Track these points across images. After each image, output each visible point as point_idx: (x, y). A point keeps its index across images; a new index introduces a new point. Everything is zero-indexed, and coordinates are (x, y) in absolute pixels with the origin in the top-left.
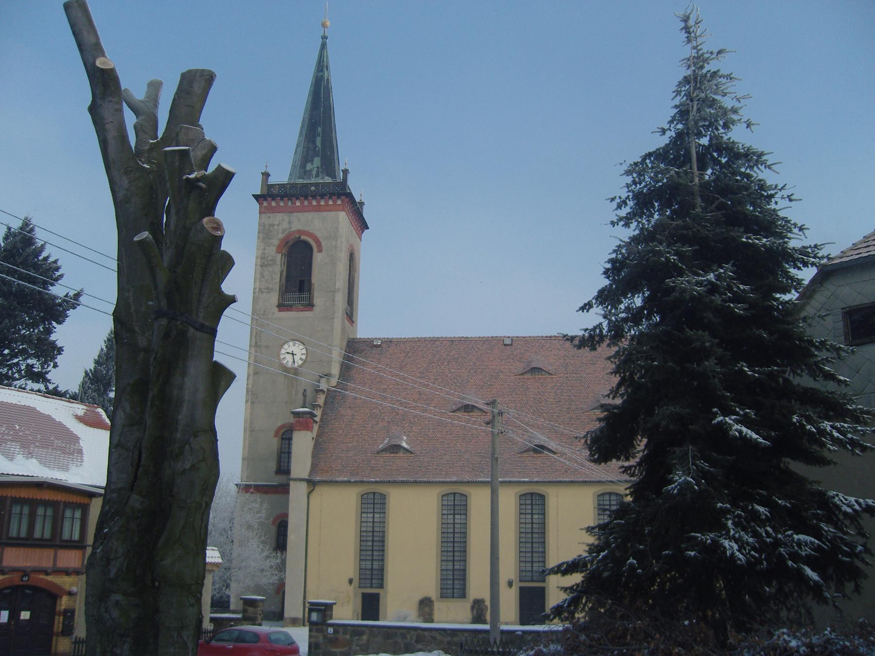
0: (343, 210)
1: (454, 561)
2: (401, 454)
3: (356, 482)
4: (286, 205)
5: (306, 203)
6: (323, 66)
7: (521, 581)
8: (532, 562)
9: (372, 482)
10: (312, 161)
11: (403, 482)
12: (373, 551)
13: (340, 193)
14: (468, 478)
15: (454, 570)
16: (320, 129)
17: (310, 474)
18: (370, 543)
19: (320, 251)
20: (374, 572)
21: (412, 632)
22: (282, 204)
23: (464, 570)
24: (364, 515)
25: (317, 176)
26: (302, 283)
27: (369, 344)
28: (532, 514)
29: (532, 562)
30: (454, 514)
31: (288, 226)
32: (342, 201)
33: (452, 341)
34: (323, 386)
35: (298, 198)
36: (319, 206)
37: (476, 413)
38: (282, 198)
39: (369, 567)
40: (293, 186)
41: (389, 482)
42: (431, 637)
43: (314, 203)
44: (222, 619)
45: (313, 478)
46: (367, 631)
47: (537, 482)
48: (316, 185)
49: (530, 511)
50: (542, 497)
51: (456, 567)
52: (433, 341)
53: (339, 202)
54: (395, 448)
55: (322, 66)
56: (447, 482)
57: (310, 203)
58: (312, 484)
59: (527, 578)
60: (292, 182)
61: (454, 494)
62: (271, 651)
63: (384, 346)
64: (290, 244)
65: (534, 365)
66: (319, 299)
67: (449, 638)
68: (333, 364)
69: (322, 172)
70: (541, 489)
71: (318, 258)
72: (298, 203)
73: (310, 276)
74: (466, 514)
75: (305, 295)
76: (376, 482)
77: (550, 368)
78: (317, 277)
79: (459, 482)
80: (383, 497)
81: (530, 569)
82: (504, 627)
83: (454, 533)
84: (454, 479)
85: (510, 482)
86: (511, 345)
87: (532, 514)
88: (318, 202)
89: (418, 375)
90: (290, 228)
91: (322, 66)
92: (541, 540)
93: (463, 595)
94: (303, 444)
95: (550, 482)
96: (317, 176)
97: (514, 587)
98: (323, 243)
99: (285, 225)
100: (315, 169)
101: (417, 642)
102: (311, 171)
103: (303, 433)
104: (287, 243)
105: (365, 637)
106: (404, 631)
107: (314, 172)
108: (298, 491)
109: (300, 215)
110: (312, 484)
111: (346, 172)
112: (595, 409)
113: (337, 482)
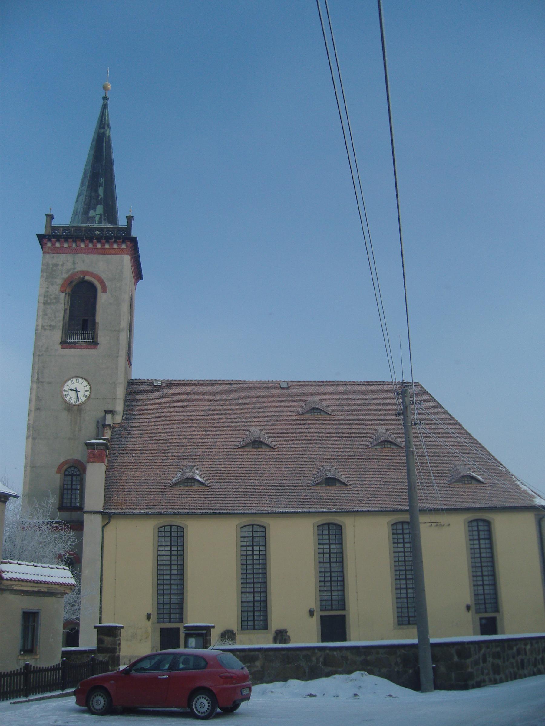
0: (127, 254)
1: (254, 592)
2: (195, 487)
3: (153, 514)
4: (70, 246)
5: (91, 245)
6: (105, 124)
7: (321, 610)
8: (331, 591)
9: (170, 514)
10: (95, 209)
11: (202, 514)
12: (170, 584)
13: (126, 239)
14: (267, 509)
15: (254, 601)
16: (102, 180)
17: (104, 507)
18: (168, 577)
19: (104, 291)
20: (173, 606)
21: (319, 653)
22: (66, 245)
23: (265, 601)
24: (160, 548)
25: (100, 222)
26: (85, 322)
27: (150, 385)
28: (329, 544)
29: (331, 591)
30: (253, 546)
31: (72, 267)
32: (127, 246)
33: (231, 383)
34: (109, 420)
35: (83, 241)
36: (103, 248)
37: (264, 449)
38: (66, 239)
39: (167, 601)
40: (78, 229)
41: (188, 514)
42: (342, 657)
43: (99, 246)
44: (70, 652)
45: (107, 511)
46: (260, 656)
47: (335, 512)
48: (101, 229)
49: (327, 541)
50: (339, 527)
51: (256, 599)
52: (213, 383)
53: (124, 246)
54: (189, 481)
55: (103, 124)
56: (246, 513)
57: (95, 246)
58: (107, 517)
59: (327, 607)
60: (75, 225)
61: (252, 525)
62: (226, 677)
63: (165, 387)
64: (74, 284)
65: (313, 406)
66: (103, 337)
67: (369, 658)
68: (118, 401)
69: (105, 219)
70: (338, 519)
71: (102, 299)
72: (82, 245)
73: (94, 314)
74: (265, 546)
75: (89, 333)
76: (175, 514)
77: (327, 409)
78: (102, 316)
79: (259, 513)
80: (182, 529)
81: (329, 598)
82: (433, 640)
83: (253, 564)
84: (253, 510)
85: (309, 512)
86: (287, 388)
87: (329, 544)
88: (103, 245)
89: (202, 414)
90: (74, 269)
91: (103, 124)
92: (339, 569)
93: (265, 627)
94: (95, 475)
95: (348, 512)
96: (100, 222)
97: (315, 617)
98: (108, 284)
99: (69, 265)
100: (98, 217)
101: (325, 664)
102: (94, 217)
103: (98, 464)
104: (71, 282)
105: (258, 663)
106: (309, 653)
107: (97, 219)
108: (92, 524)
109: (84, 256)
110: (107, 517)
111: (130, 219)
112: (377, 445)
113: (134, 514)
